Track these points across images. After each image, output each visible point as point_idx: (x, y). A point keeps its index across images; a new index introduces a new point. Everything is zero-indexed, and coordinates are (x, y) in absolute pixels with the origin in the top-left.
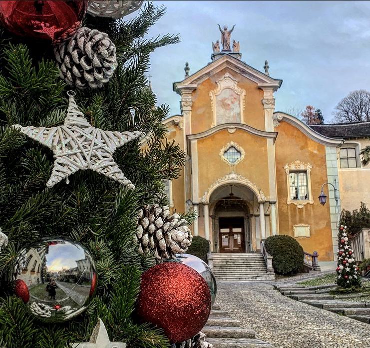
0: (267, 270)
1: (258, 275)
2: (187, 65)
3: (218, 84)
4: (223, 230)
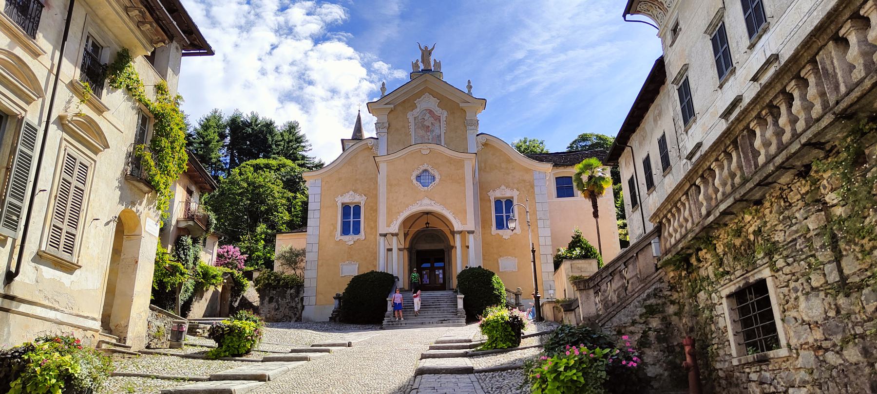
0: (456, 313)
1: (446, 319)
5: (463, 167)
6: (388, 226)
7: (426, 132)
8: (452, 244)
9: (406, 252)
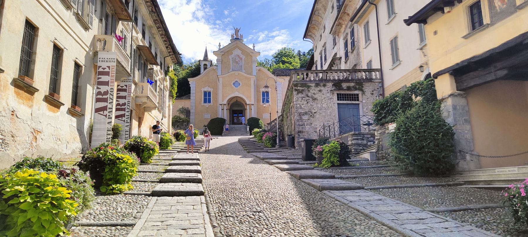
0: (247, 132)
2: (220, 44)
4: (234, 115)
5: (250, 80)
6: (223, 101)
7: (237, 64)
8: (246, 108)
9: (228, 110)
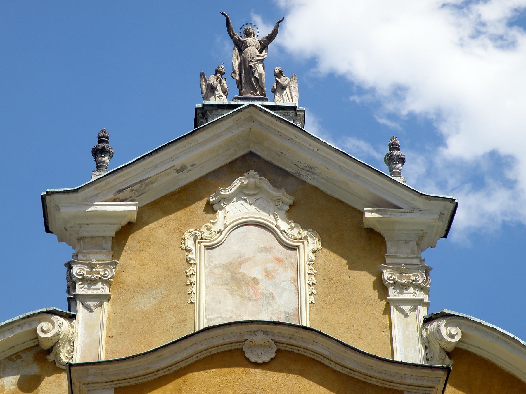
3: (215, 207)
